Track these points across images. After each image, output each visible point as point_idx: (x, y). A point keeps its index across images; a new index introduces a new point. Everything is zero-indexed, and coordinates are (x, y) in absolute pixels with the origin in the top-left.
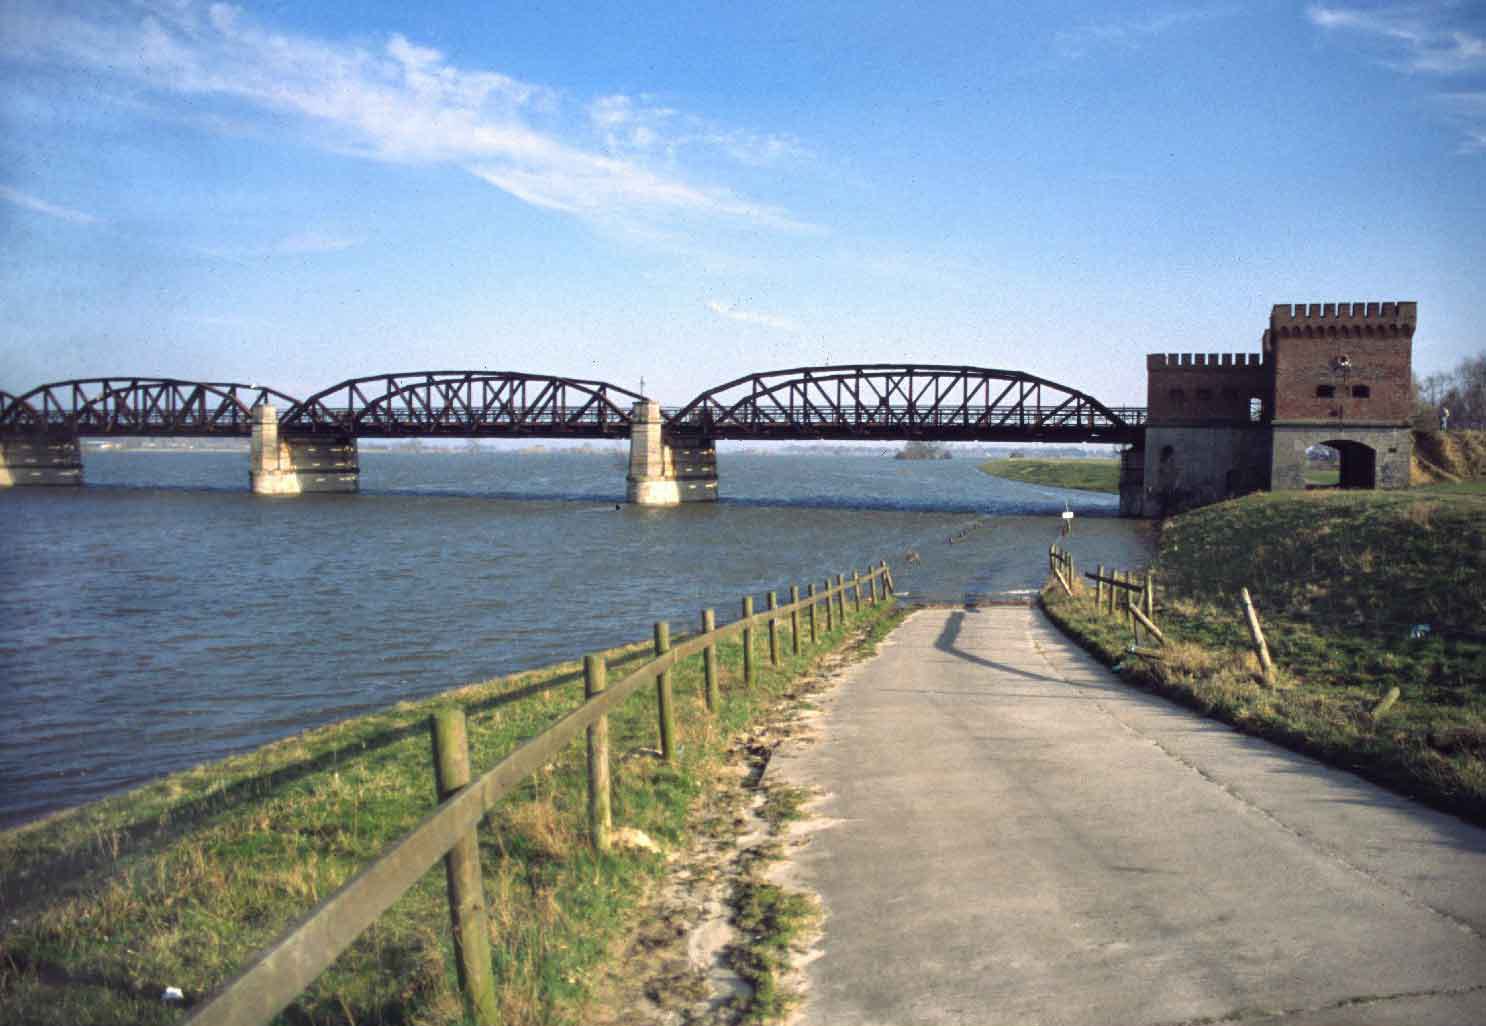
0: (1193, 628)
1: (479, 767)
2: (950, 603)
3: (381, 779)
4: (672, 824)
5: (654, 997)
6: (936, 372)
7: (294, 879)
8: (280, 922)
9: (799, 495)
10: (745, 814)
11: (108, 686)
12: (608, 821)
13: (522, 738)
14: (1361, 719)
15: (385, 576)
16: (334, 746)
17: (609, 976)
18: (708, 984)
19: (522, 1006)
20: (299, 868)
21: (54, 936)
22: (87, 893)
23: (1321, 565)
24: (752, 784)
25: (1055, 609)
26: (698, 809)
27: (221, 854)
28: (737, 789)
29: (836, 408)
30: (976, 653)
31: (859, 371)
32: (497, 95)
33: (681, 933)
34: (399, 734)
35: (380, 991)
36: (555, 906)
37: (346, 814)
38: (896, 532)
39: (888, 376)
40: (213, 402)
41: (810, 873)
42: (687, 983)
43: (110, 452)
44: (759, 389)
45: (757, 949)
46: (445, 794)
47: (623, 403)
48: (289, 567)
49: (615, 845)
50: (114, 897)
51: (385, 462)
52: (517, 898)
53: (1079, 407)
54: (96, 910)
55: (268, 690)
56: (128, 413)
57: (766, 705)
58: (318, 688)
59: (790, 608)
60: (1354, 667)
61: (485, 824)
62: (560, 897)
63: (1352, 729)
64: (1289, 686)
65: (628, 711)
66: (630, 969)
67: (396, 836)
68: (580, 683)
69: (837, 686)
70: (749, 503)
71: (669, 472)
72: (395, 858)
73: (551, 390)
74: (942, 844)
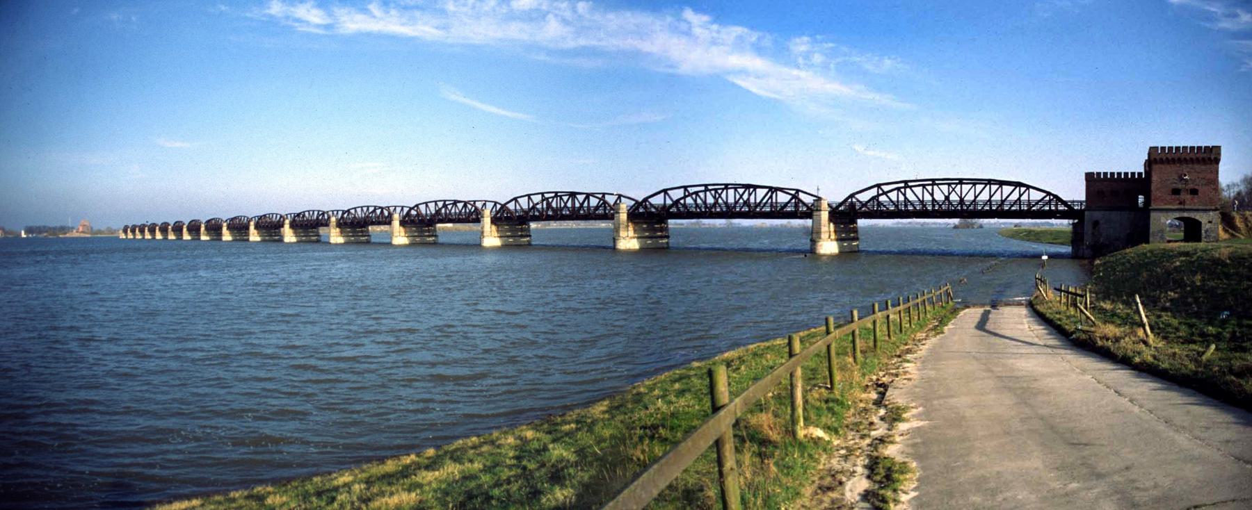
0: (1109, 317)
1: (734, 395)
2: (983, 305)
3: (682, 402)
4: (836, 425)
6: (974, 182)
9: (902, 248)
10: (875, 419)
12: (802, 423)
13: (756, 379)
14: (1196, 361)
15: (683, 293)
17: (803, 506)
23: (1175, 282)
24: (879, 403)
25: (1038, 307)
26: (850, 417)
28: (871, 406)
29: (922, 202)
30: (998, 331)
31: (934, 182)
32: (740, 38)
33: (841, 483)
36: (774, 469)
37: (664, 419)
38: (954, 267)
39: (949, 185)
41: (910, 450)
44: (881, 192)
45: (882, 492)
46: (716, 409)
47: (808, 200)
49: (805, 436)
51: (681, 232)
52: (753, 464)
53: (1050, 200)
57: (886, 361)
59: (898, 308)
60: (1192, 334)
61: (736, 424)
62: (776, 464)
63: (1192, 366)
64: (1160, 345)
65: (812, 364)
66: (814, 503)
67: (689, 431)
68: (787, 350)
69: (924, 350)
70: (876, 253)
71: (833, 236)
72: (689, 443)
73: (770, 194)
74: (980, 433)
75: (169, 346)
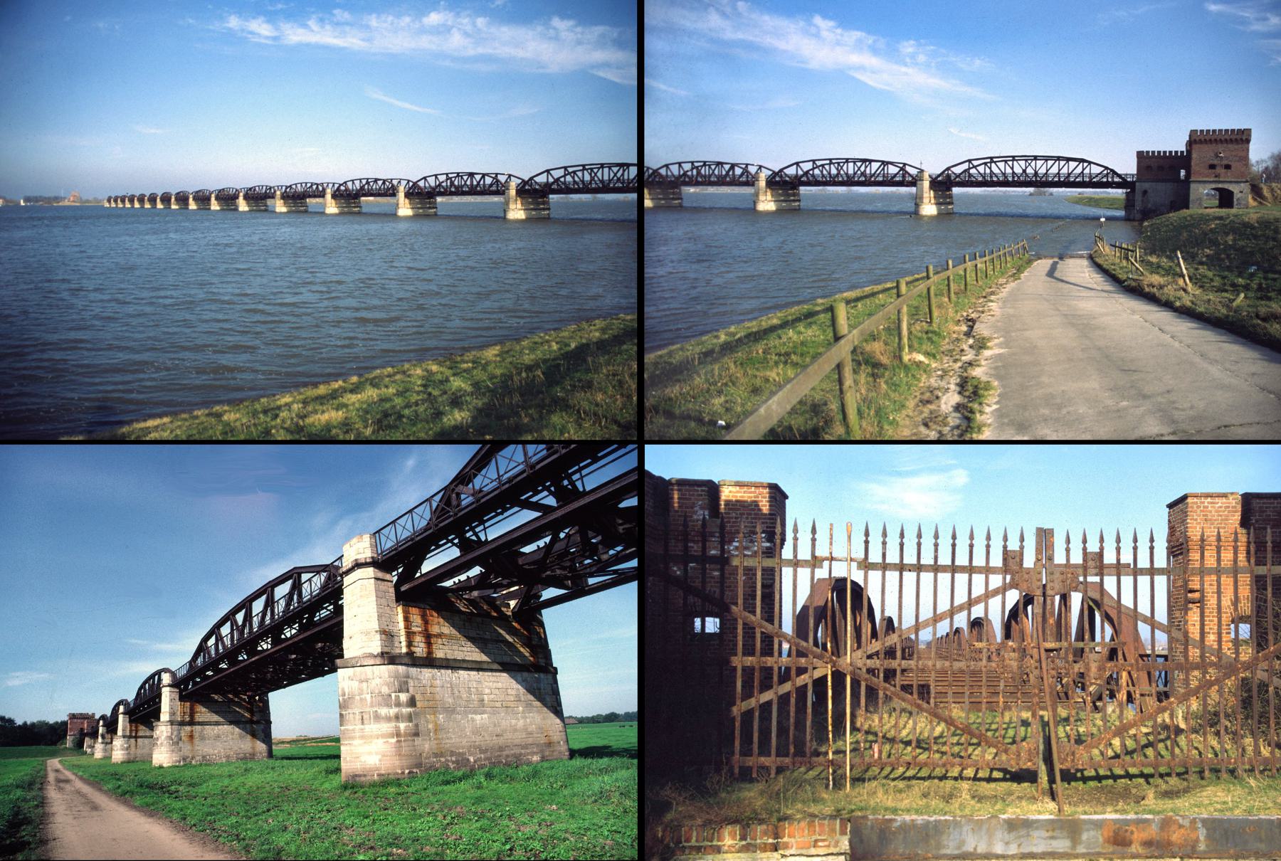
0: (1156, 269)
1: (852, 327)
2: (1052, 257)
3: (810, 332)
4: (934, 351)
5: (926, 425)
6: (1046, 159)
7: (772, 375)
8: (767, 393)
9: (988, 211)
10: (965, 347)
11: (694, 293)
12: (907, 350)
13: (870, 315)
14: (1228, 306)
15: (812, 246)
16: (790, 318)
17: (907, 416)
18: (949, 419)
19: (870, 429)
20: (775, 370)
21: (670, 399)
22: (685, 380)
23: (1210, 241)
24: (968, 334)
25: (1097, 260)
26: (945, 345)
27: (741, 364)
28: (962, 336)
29: (1004, 174)
30: (1064, 278)
31: (1014, 158)
32: (859, 41)
33: (938, 398)
34: (817, 313)
35: (809, 422)
36: (884, 386)
37: (795, 347)
38: (1029, 227)
39: (1026, 160)
40: (738, 171)
41: (993, 372)
42: (940, 419)
43: (694, 193)
45: (970, 405)
46: (837, 338)
47: (913, 172)
48: (770, 242)
49: (910, 360)
50: (696, 382)
51: (813, 197)
52: (868, 383)
54: (688, 388)
55: (762, 294)
56: (702, 176)
57: (974, 300)
58: (782, 293)
59: (984, 259)
60: (1225, 284)
61: (854, 351)
62: (886, 382)
63: (1224, 311)
64: (1197, 292)
65: (915, 303)
66: (916, 413)
67: (816, 357)
68: (895, 291)
69: (1004, 292)
70: (967, 214)
71: (933, 201)
72: (816, 366)
74: (1050, 359)
75: (145, 294)
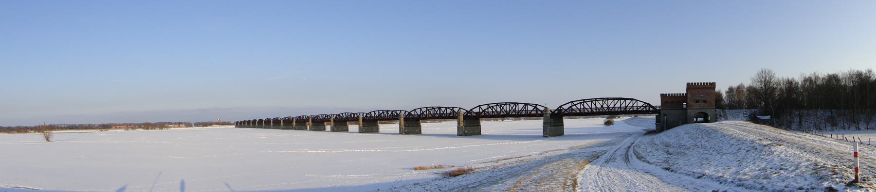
53: (646, 106)
